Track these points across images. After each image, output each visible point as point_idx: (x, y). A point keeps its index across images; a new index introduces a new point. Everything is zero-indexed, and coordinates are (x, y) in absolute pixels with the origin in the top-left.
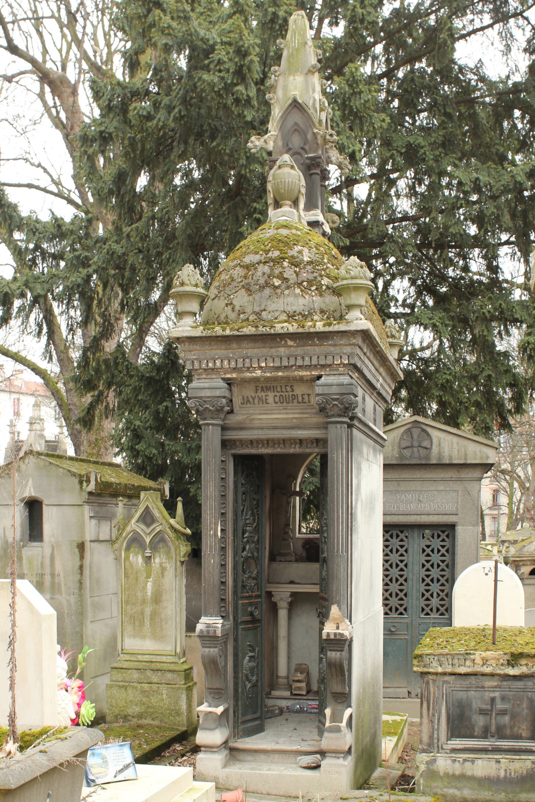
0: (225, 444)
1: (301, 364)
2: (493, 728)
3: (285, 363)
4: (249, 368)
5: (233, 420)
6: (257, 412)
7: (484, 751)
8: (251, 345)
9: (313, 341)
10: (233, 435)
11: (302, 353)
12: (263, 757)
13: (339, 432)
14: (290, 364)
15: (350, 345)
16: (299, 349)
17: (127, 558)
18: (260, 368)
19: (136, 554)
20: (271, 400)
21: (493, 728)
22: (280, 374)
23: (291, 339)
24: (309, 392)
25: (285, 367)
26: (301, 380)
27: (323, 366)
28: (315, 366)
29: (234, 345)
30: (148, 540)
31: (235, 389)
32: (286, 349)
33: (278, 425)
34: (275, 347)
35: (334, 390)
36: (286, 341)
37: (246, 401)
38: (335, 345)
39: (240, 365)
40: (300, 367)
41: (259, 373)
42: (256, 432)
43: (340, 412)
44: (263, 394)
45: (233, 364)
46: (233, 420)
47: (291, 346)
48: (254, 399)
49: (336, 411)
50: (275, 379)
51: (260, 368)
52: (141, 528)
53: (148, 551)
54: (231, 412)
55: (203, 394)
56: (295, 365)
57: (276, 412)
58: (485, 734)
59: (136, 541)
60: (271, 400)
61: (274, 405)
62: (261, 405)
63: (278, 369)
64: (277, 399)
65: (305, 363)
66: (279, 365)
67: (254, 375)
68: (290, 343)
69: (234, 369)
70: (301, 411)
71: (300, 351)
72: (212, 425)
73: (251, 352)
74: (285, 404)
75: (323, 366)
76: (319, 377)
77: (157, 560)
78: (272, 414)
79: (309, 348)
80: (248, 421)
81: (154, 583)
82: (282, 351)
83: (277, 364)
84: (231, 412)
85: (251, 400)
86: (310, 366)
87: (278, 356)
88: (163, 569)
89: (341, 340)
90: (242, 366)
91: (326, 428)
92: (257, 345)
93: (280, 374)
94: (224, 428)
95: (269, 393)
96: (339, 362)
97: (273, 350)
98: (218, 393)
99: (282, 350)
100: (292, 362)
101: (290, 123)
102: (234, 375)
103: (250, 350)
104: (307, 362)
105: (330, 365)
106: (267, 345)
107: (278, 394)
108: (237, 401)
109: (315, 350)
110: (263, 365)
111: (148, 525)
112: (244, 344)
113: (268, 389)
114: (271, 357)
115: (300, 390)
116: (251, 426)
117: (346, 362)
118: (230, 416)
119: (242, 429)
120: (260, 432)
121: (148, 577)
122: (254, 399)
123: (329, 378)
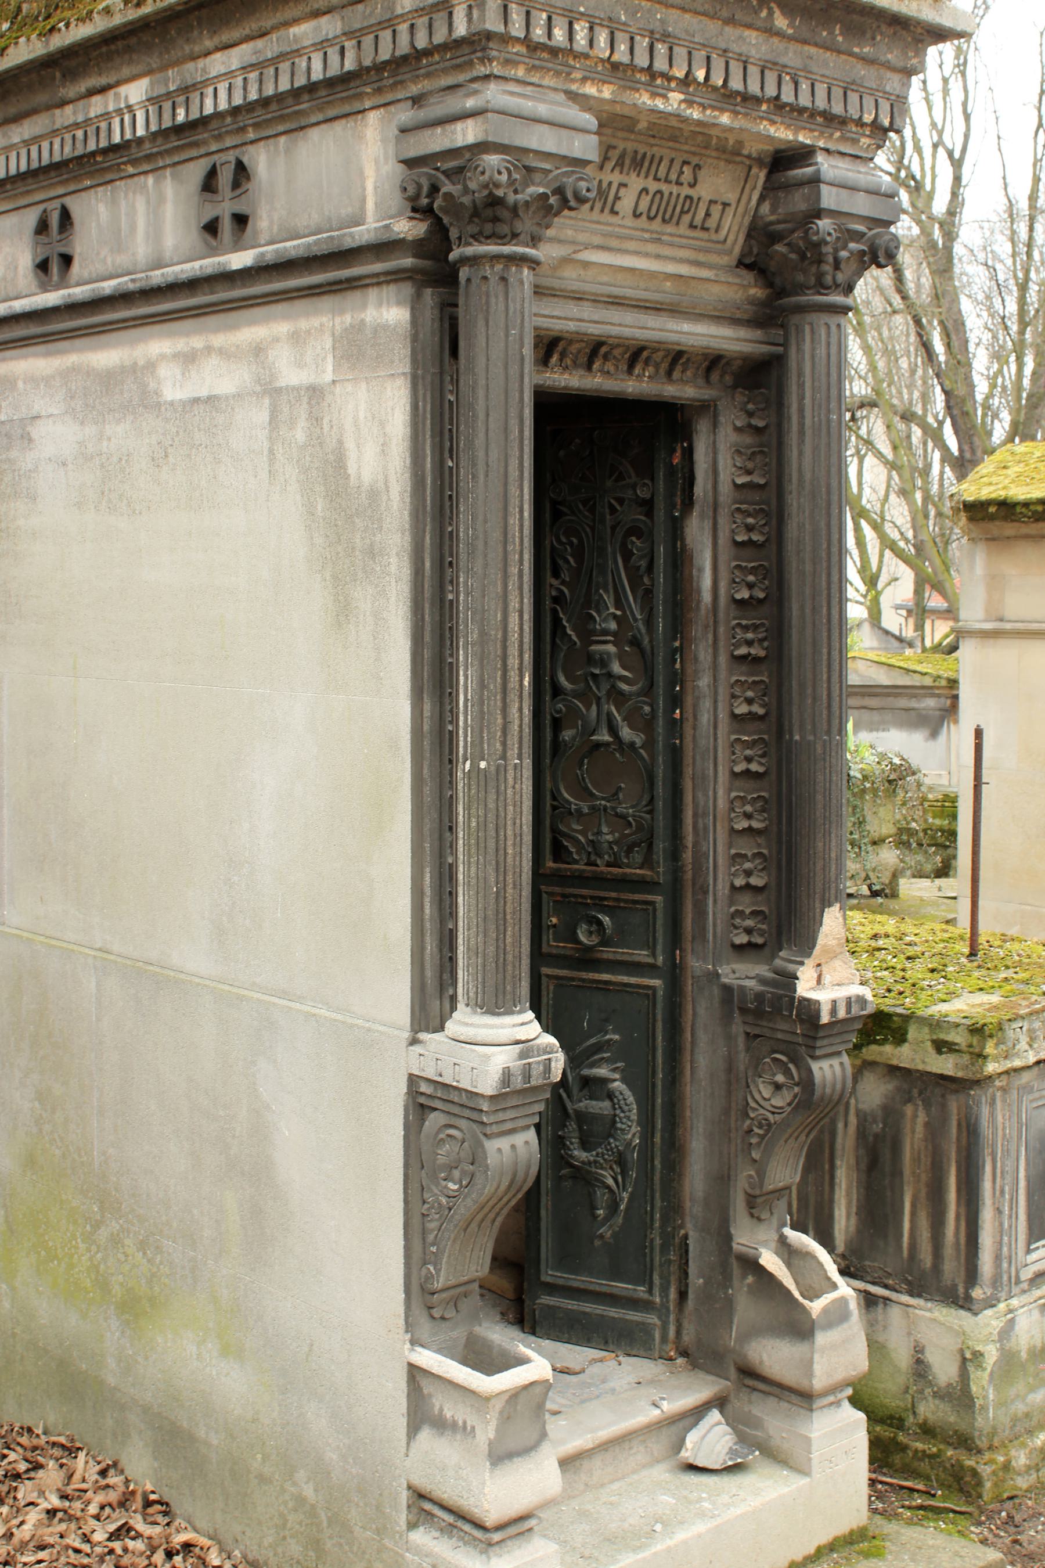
16: (793, 47)
18: (687, 81)
24: (731, 197)
27: (831, 120)
33: (629, 293)
36: (771, 13)
42: (573, 309)
44: (616, 178)
47: (779, 34)
57: (632, 245)
61: (629, 222)
67: (659, 104)
71: (791, 55)
74: (656, 225)
75: (831, 120)
79: (813, 50)
93: (725, 119)
99: (752, 36)
107: (653, 186)
116: (556, 283)
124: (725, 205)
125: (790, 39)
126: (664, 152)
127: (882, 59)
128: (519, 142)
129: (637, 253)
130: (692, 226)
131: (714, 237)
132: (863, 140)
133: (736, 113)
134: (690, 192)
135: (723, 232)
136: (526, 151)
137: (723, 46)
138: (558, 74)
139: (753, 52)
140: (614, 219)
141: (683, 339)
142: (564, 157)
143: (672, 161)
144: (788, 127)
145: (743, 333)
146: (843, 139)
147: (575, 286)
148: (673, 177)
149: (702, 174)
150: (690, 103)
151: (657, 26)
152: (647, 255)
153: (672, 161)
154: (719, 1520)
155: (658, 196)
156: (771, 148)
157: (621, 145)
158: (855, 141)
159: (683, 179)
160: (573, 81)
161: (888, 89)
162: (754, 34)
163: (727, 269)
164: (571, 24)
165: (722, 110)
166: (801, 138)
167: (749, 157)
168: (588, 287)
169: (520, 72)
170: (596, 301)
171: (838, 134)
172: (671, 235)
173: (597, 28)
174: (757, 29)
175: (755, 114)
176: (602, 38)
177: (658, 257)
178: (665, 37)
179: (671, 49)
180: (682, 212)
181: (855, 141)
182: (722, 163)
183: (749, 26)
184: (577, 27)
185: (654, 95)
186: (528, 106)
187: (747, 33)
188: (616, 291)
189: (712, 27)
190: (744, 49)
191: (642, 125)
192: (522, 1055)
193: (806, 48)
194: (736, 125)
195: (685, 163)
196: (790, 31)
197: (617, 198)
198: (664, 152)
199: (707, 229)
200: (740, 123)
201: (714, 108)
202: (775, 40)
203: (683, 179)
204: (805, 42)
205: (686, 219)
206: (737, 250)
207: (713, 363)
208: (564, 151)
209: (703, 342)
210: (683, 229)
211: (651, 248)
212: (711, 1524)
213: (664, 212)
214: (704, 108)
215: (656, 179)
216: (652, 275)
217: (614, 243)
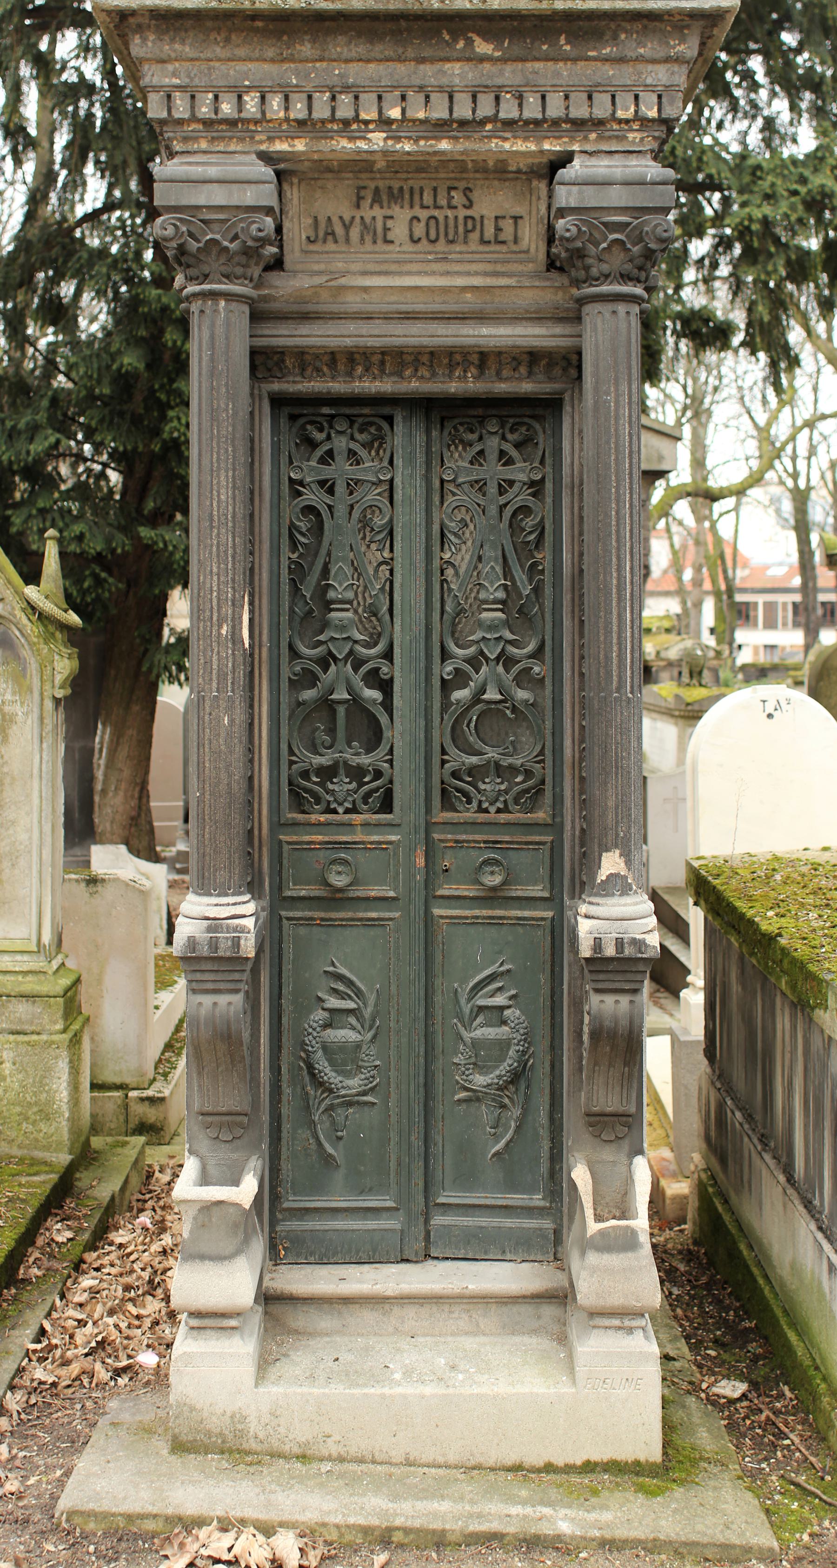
0: (263, 362)
1: (514, 114)
3: (463, 111)
4: (346, 123)
5: (284, 287)
6: (354, 267)
8: (360, 49)
9: (554, 44)
11: (518, 80)
13: (623, 326)
14: (481, 113)
15: (667, 60)
16: (509, 68)
18: (384, 122)
20: (399, 231)
22: (444, 145)
23: (486, 36)
25: (463, 123)
26: (500, 171)
27: (579, 124)
28: (556, 123)
29: (306, 49)
31: (293, 194)
32: (467, 66)
34: (432, 60)
35: (616, 197)
36: (470, 42)
37: (323, 233)
38: (621, 60)
39: (321, 111)
40: (509, 124)
41: (378, 139)
42: (351, 327)
43: (628, 267)
44: (378, 212)
45: (299, 110)
46: (284, 287)
47: (483, 59)
48: (347, 227)
49: (617, 261)
50: (419, 166)
51: (384, 122)
54: (277, 264)
55: (201, 197)
56: (494, 119)
57: (414, 267)
60: (399, 231)
61: (409, 247)
62: (369, 246)
63: (441, 127)
64: (419, 230)
65: (527, 114)
66: (445, 115)
67: (362, 145)
68: (483, 47)
69: (301, 123)
70: (489, 268)
71: (509, 74)
72: (229, 296)
73: (355, 73)
76: (566, 159)
78: (401, 274)
79: (538, 65)
80: (325, 295)
82: (456, 72)
83: (440, 112)
84: (277, 264)
85: (339, 230)
86: (537, 123)
87: (441, 89)
89: (640, 44)
90: (327, 114)
91: (578, 319)
92: (379, 49)
93: (444, 145)
94: (258, 316)
95: (396, 210)
96: (630, 113)
97: (427, 69)
98: (249, 196)
100: (485, 108)
102: (300, 146)
103: (354, 67)
104: (532, 111)
105: (599, 123)
106: (410, 53)
107: (424, 214)
108: (296, 231)
109: (558, 74)
110: (395, 113)
112: (339, 47)
113: (395, 196)
114: (421, 88)
115: (491, 203)
116: (335, 308)
117: (653, 113)
118: (276, 279)
119: (305, 317)
120: (365, 328)
122: (347, 227)
123: (593, 161)
124: (516, 219)
125: (504, 60)
126: (422, 183)
127: (631, 54)
128: (193, 202)
129: (419, 273)
130: (483, 242)
131: (515, 248)
132: (631, 136)
133: (456, 138)
134: (469, 213)
135: (524, 243)
136: (198, 208)
137: (418, 82)
138: (241, 140)
139: (457, 81)
140: (390, 247)
141: (482, 341)
142: (238, 207)
143: (435, 190)
144: (526, 139)
145: (558, 330)
146: (600, 138)
147: (355, 307)
148: (443, 202)
149: (475, 196)
150: (398, 139)
151: (335, 81)
152: (433, 273)
153: (435, 190)
154: (451, 1391)
155: (432, 223)
156: (545, 160)
157: (372, 185)
158: (622, 138)
159: (454, 202)
160: (261, 142)
161: (649, 81)
162: (458, 65)
163: (536, 275)
164: (240, 97)
165: (438, 139)
166: (547, 146)
167: (519, 171)
168: (370, 308)
169: (204, 145)
170: (387, 317)
171: (593, 136)
172: (460, 253)
173: (268, 96)
174: (458, 60)
175: (476, 136)
176: (275, 103)
177: (448, 273)
178: (346, 89)
179: (356, 98)
180: (467, 232)
181: (622, 138)
182: (496, 183)
183: (448, 60)
184: (246, 98)
185: (352, 139)
186: (198, 171)
187: (448, 66)
188: (404, 307)
189: (402, 69)
190: (444, 81)
191: (381, 164)
192: (209, 929)
193: (529, 65)
194: (460, 147)
195: (450, 189)
196: (497, 54)
197: (386, 229)
198: (422, 183)
199: (503, 242)
200: (463, 145)
201: (427, 138)
202: (487, 66)
203: (454, 202)
204: (523, 60)
205: (475, 236)
206: (542, 256)
207: (533, 358)
208: (235, 202)
209: (510, 342)
210: (474, 246)
211: (435, 267)
212: (441, 1390)
213: (437, 234)
214: (416, 141)
215: (423, 207)
216: (431, 289)
217: (393, 267)
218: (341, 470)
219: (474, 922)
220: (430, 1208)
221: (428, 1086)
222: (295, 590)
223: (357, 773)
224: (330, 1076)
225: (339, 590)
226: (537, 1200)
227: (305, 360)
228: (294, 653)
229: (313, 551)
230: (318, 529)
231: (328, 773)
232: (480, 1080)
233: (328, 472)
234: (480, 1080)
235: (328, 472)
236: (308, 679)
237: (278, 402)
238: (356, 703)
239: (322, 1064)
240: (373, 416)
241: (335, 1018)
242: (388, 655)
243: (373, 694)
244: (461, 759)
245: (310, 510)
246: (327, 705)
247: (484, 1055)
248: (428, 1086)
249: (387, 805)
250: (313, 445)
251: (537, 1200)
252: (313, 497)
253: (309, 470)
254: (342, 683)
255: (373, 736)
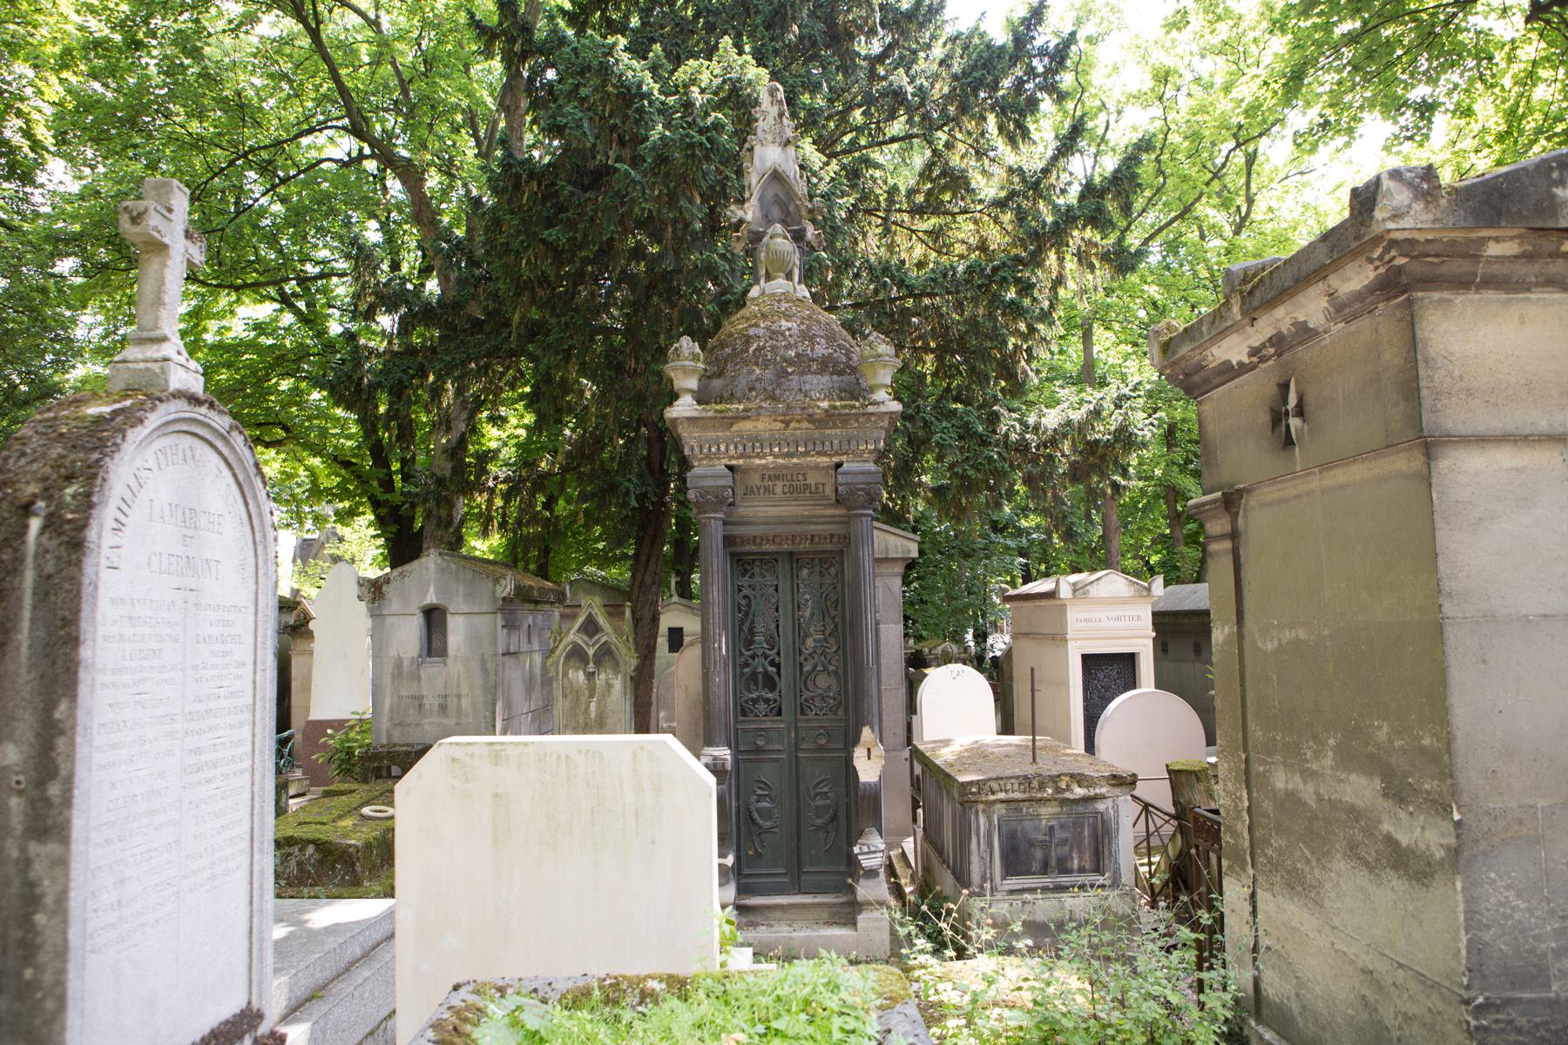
0: (728, 540)
2: (1053, 862)
7: (1045, 889)
10: (736, 531)
12: (778, 914)
17: (565, 674)
19: (577, 669)
21: (1053, 862)
30: (591, 652)
52: (581, 639)
53: (592, 664)
58: (1045, 870)
59: (577, 654)
77: (603, 676)
81: (599, 703)
88: (609, 686)
94: (725, 523)
101: (770, 194)
111: (591, 636)
121: (591, 696)
218: (758, 579)
219: (815, 759)
220: (800, 872)
221: (799, 826)
222: (741, 629)
223: (767, 701)
224: (760, 821)
225: (759, 628)
226: (842, 868)
227: (744, 540)
228: (741, 654)
229: (747, 614)
230: (749, 605)
231: (755, 701)
232: (818, 822)
233: (753, 581)
234: (818, 822)
235: (753, 581)
236: (747, 665)
237: (732, 555)
238: (766, 674)
239: (756, 815)
240: (769, 561)
241: (760, 798)
242: (778, 654)
243: (772, 669)
244: (806, 694)
245: (745, 597)
246: (754, 675)
247: (820, 811)
248: (799, 826)
249: (779, 713)
250: (746, 571)
251: (842, 868)
252: (745, 592)
253: (745, 581)
254: (760, 665)
255: (771, 684)
